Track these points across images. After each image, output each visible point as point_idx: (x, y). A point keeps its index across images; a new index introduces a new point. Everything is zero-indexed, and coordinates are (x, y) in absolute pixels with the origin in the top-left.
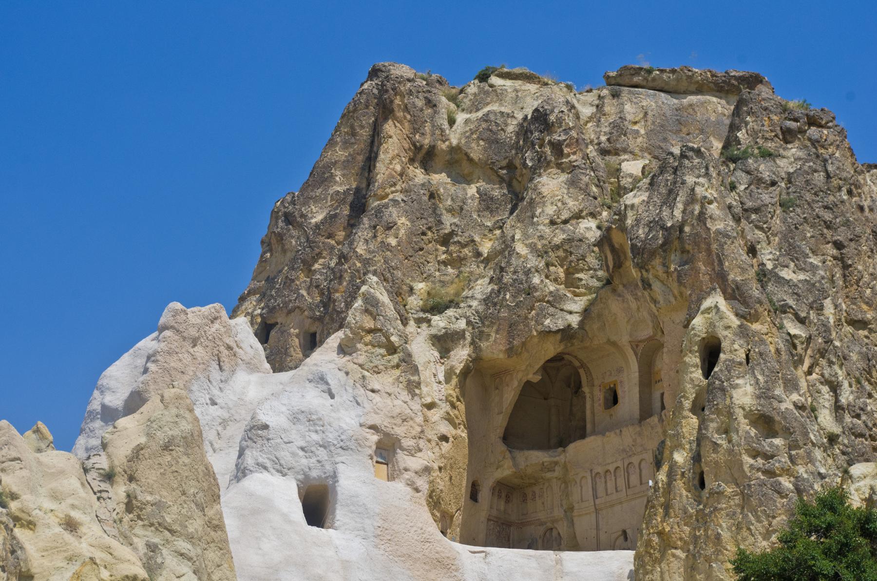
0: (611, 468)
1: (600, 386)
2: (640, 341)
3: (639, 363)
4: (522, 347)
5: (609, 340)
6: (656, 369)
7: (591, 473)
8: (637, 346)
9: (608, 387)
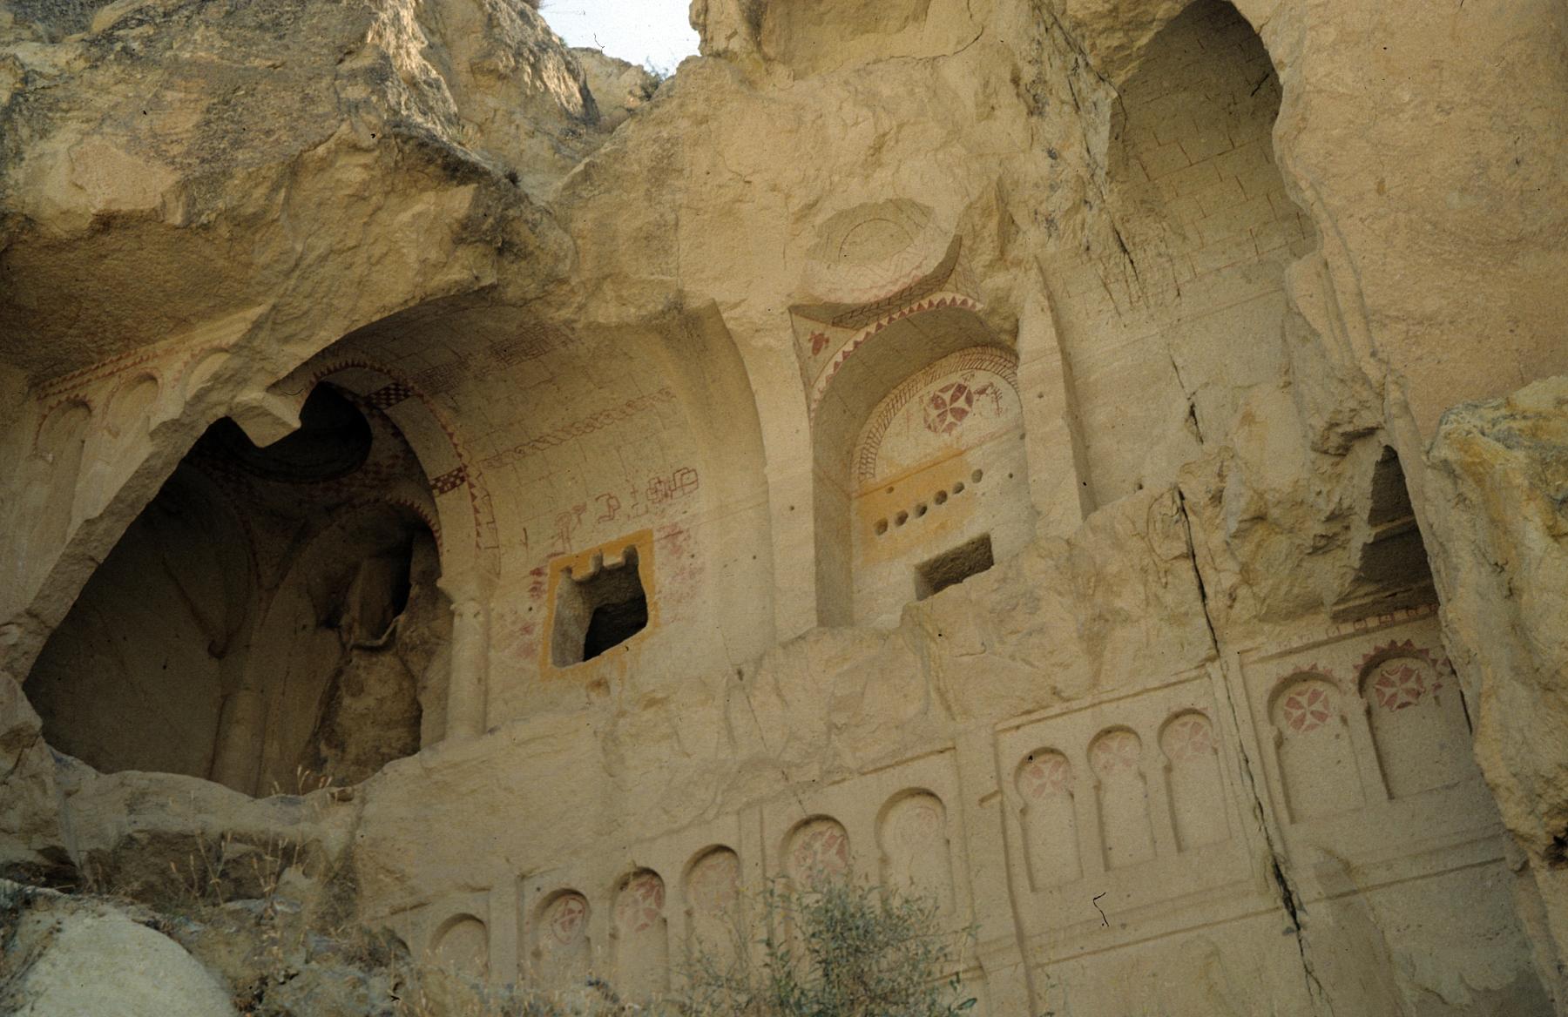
0: (669, 863)
1: (538, 572)
2: (845, 316)
3: (817, 423)
4: (275, 189)
5: (677, 306)
6: (883, 472)
7: (521, 896)
8: (819, 343)
9: (591, 569)
